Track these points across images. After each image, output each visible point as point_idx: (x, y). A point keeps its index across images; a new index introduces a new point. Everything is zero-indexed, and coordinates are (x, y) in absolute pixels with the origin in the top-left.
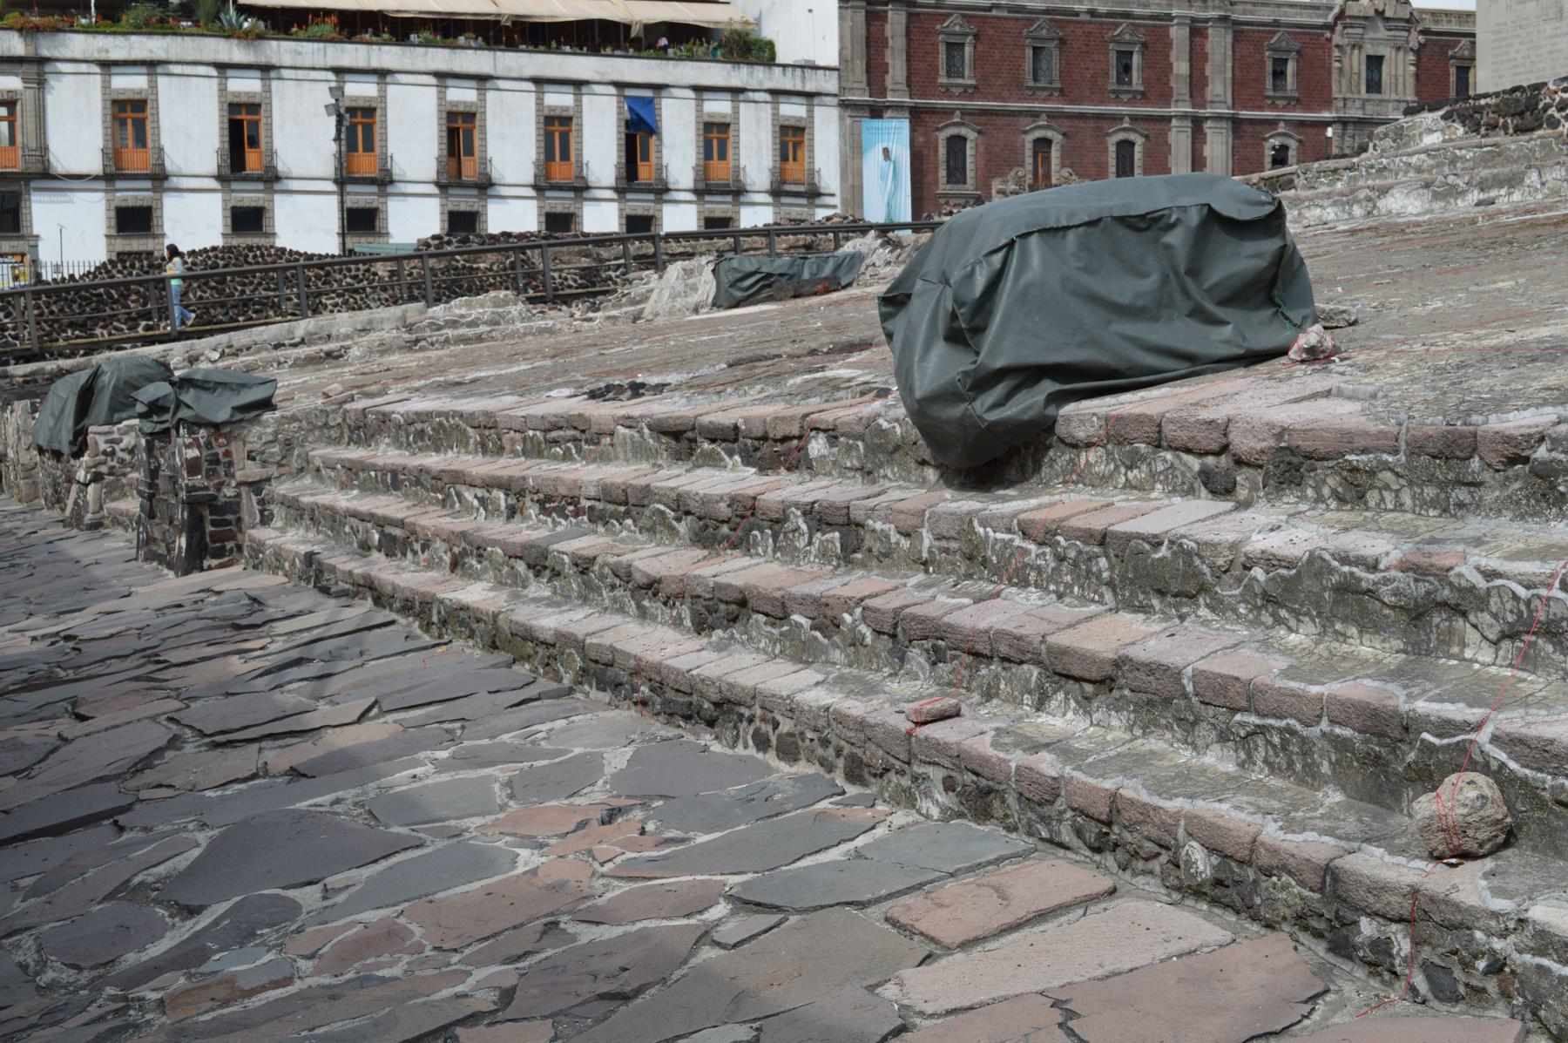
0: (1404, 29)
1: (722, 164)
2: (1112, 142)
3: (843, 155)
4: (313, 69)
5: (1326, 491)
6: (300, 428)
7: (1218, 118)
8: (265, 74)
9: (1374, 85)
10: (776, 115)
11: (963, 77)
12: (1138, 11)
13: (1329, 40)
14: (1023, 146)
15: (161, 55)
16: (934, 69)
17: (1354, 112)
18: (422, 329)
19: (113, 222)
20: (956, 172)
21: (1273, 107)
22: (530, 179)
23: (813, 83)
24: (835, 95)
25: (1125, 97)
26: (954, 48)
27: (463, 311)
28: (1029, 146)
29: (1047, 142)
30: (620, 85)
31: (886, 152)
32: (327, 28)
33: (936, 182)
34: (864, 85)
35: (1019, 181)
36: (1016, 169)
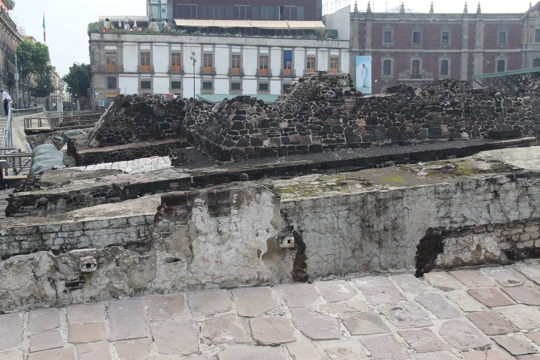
4: (195, 43)
7: (478, 52)
10: (329, 55)
11: (390, 42)
12: (450, 20)
14: (409, 63)
15: (153, 40)
19: (140, 86)
20: (387, 71)
21: (499, 48)
22: (255, 74)
23: (342, 45)
29: (418, 61)
30: (282, 47)
31: (364, 65)
32: (199, 32)
33: (380, 74)
36: (407, 70)
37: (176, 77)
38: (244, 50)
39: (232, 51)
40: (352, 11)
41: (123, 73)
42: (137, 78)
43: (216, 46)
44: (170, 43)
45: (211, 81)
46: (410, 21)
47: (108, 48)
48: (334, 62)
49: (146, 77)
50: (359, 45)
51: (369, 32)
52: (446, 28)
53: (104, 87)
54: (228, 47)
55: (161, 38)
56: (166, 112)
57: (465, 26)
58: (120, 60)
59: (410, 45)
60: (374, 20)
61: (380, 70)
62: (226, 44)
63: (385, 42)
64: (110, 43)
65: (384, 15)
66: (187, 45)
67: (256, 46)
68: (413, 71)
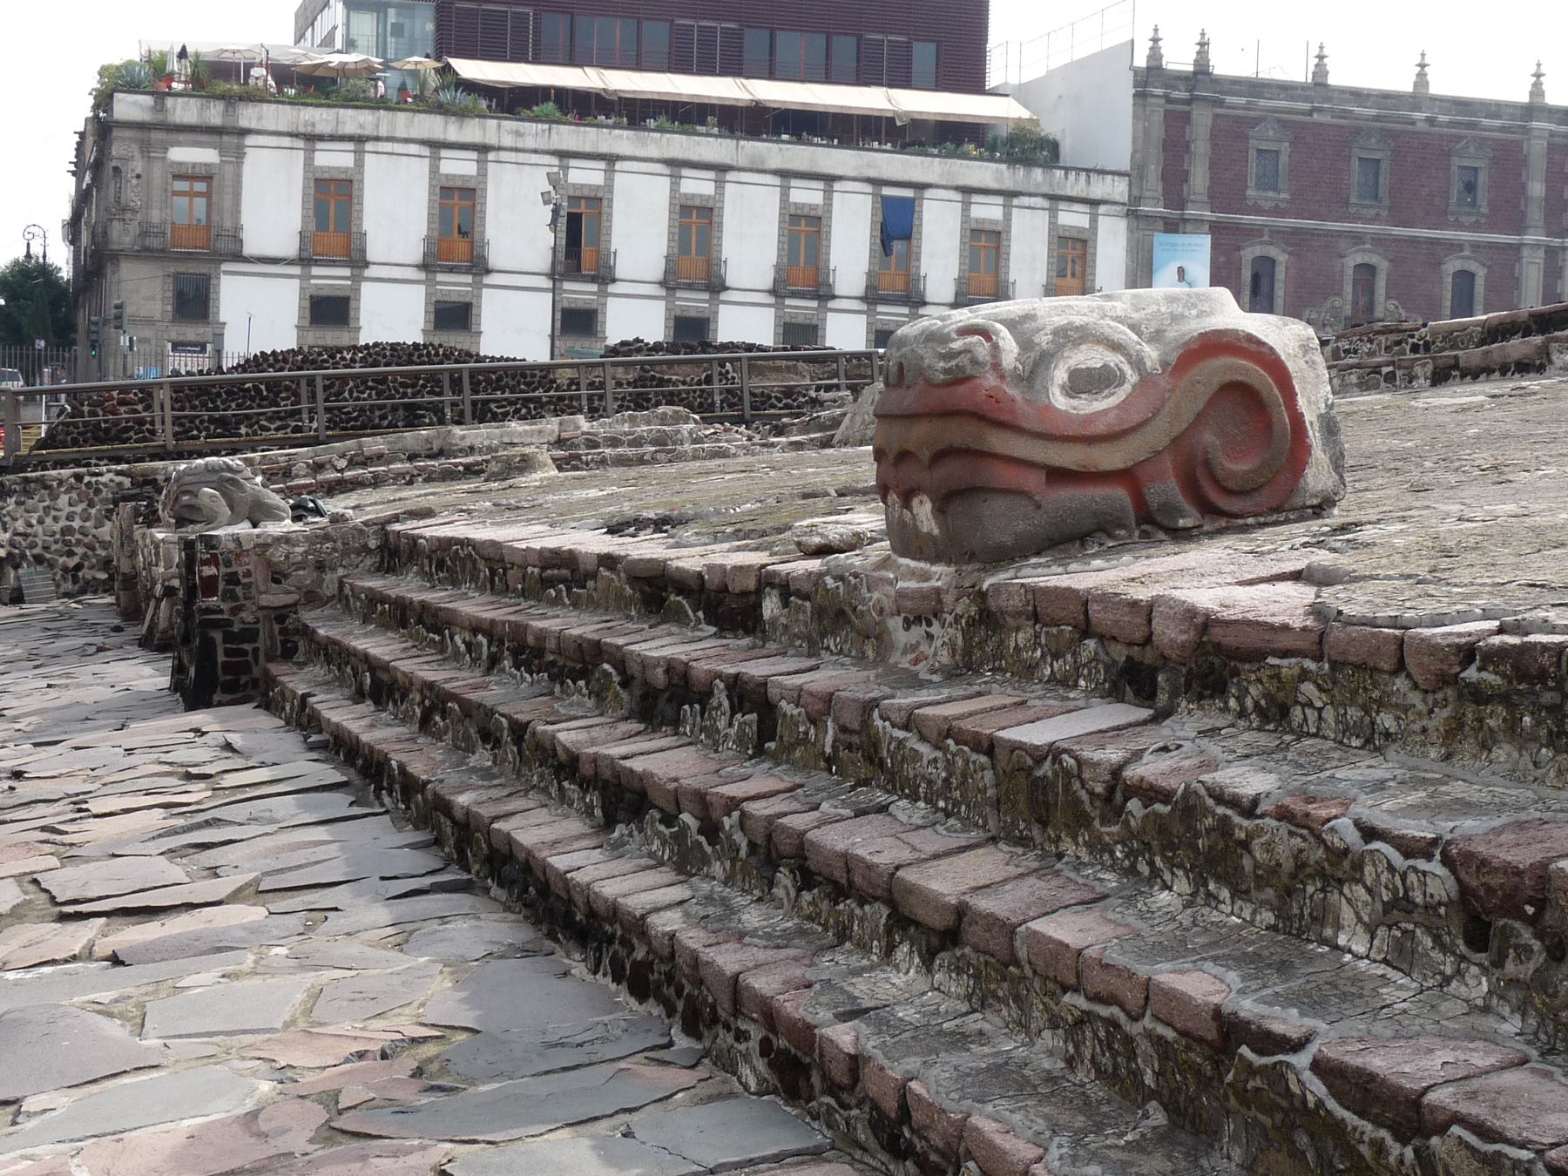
4: (535, 151)
5: (1249, 703)
6: (334, 550)
8: (482, 156)
10: (1053, 225)
11: (1275, 189)
12: (1486, 122)
14: (1342, 272)
18: (577, 446)
19: (307, 313)
23: (1100, 188)
24: (1124, 204)
27: (626, 428)
28: (1350, 272)
30: (877, 183)
32: (550, 107)
37: (454, 285)
38: (729, 188)
39: (683, 190)
40: (1141, 61)
41: (238, 257)
42: (296, 282)
43: (618, 166)
44: (436, 145)
45: (594, 306)
46: (1345, 114)
47: (183, 154)
48: (1070, 253)
49: (330, 278)
50: (1165, 193)
51: (1201, 147)
52: (1472, 150)
53: (158, 316)
54: (667, 171)
55: (402, 123)
57: (1537, 149)
58: (227, 204)
59: (1347, 204)
60: (1220, 103)
62: (658, 161)
63: (1258, 187)
64: (191, 137)
65: (1256, 87)
66: (504, 156)
67: (776, 172)
68: (1355, 303)
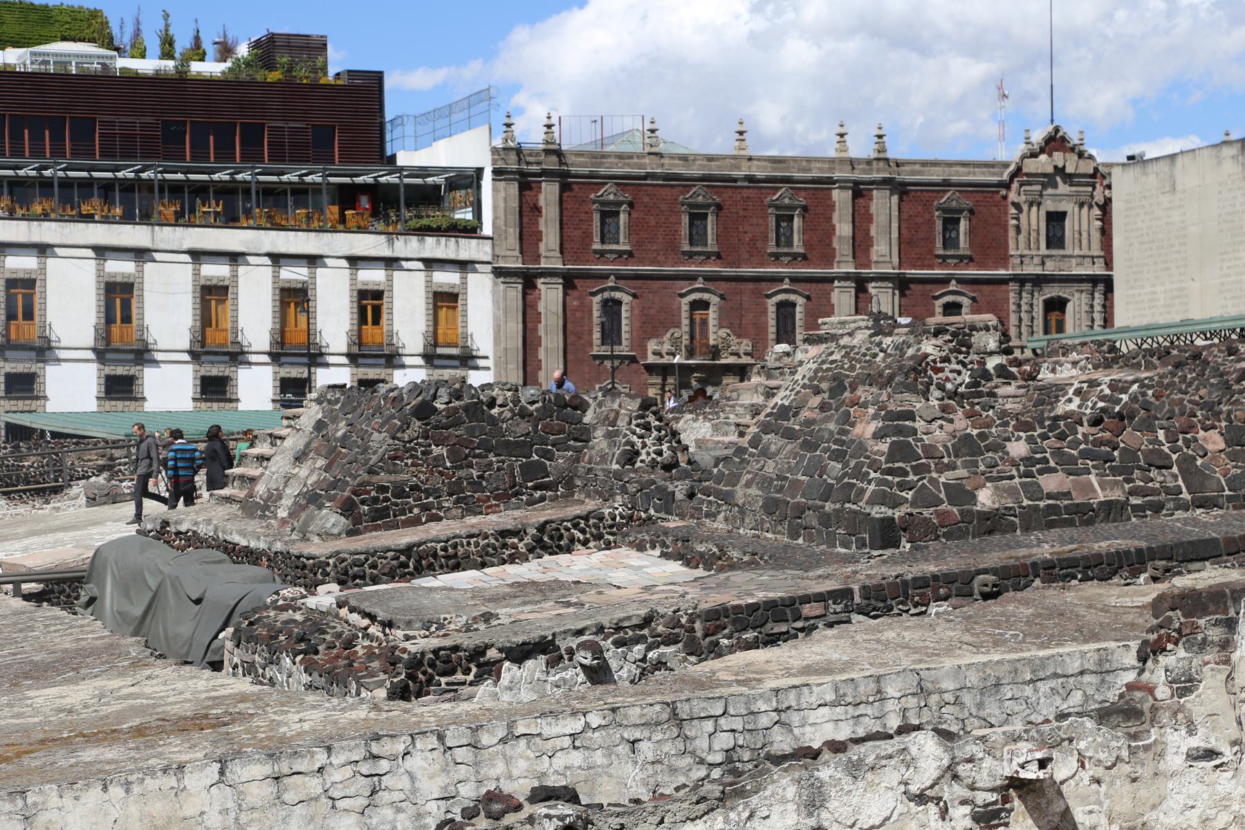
0: (1087, 185)
1: (376, 330)
2: (771, 303)
3: (496, 318)
9: (1055, 240)
10: (429, 282)
11: (618, 243)
12: (797, 175)
13: (1005, 198)
14: (680, 308)
16: (588, 236)
17: (1032, 269)
20: (611, 333)
24: (488, 263)
25: (786, 260)
26: (609, 214)
28: (685, 308)
34: (517, 253)
35: (675, 342)
36: (672, 331)
39: (107, 270)
56: (536, 431)
60: (567, 174)
61: (591, 333)
